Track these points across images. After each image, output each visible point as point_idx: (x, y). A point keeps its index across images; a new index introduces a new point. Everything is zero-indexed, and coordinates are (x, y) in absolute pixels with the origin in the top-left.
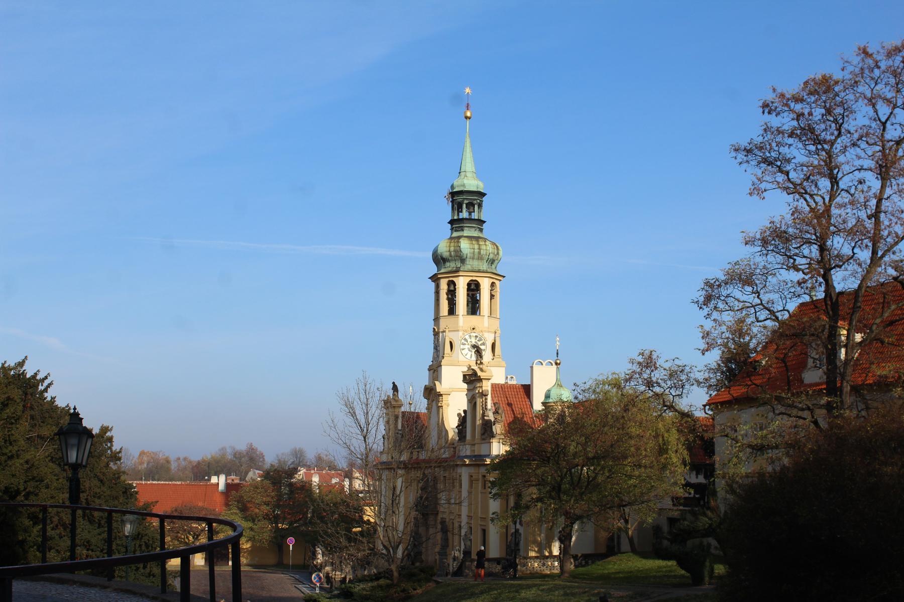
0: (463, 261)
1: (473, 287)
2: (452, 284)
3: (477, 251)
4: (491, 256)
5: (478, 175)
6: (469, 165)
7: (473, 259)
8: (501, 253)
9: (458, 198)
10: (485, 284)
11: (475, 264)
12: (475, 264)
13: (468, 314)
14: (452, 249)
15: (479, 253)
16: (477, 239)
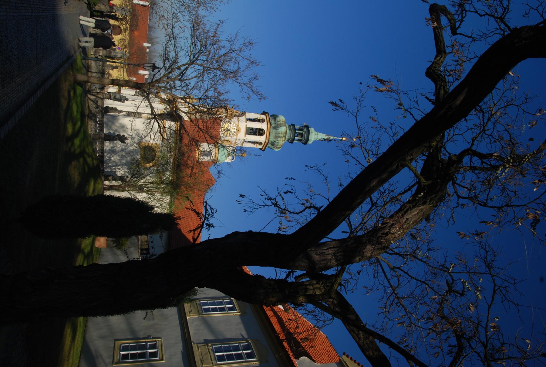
0: (275, 128)
1: (261, 132)
2: (263, 121)
3: (280, 135)
4: (276, 144)
5: (315, 142)
6: (322, 136)
7: (276, 133)
8: (277, 150)
9: (305, 129)
10: (262, 139)
11: (273, 134)
12: (273, 134)
13: (247, 128)
14: (281, 122)
15: (279, 137)
16: (285, 136)
